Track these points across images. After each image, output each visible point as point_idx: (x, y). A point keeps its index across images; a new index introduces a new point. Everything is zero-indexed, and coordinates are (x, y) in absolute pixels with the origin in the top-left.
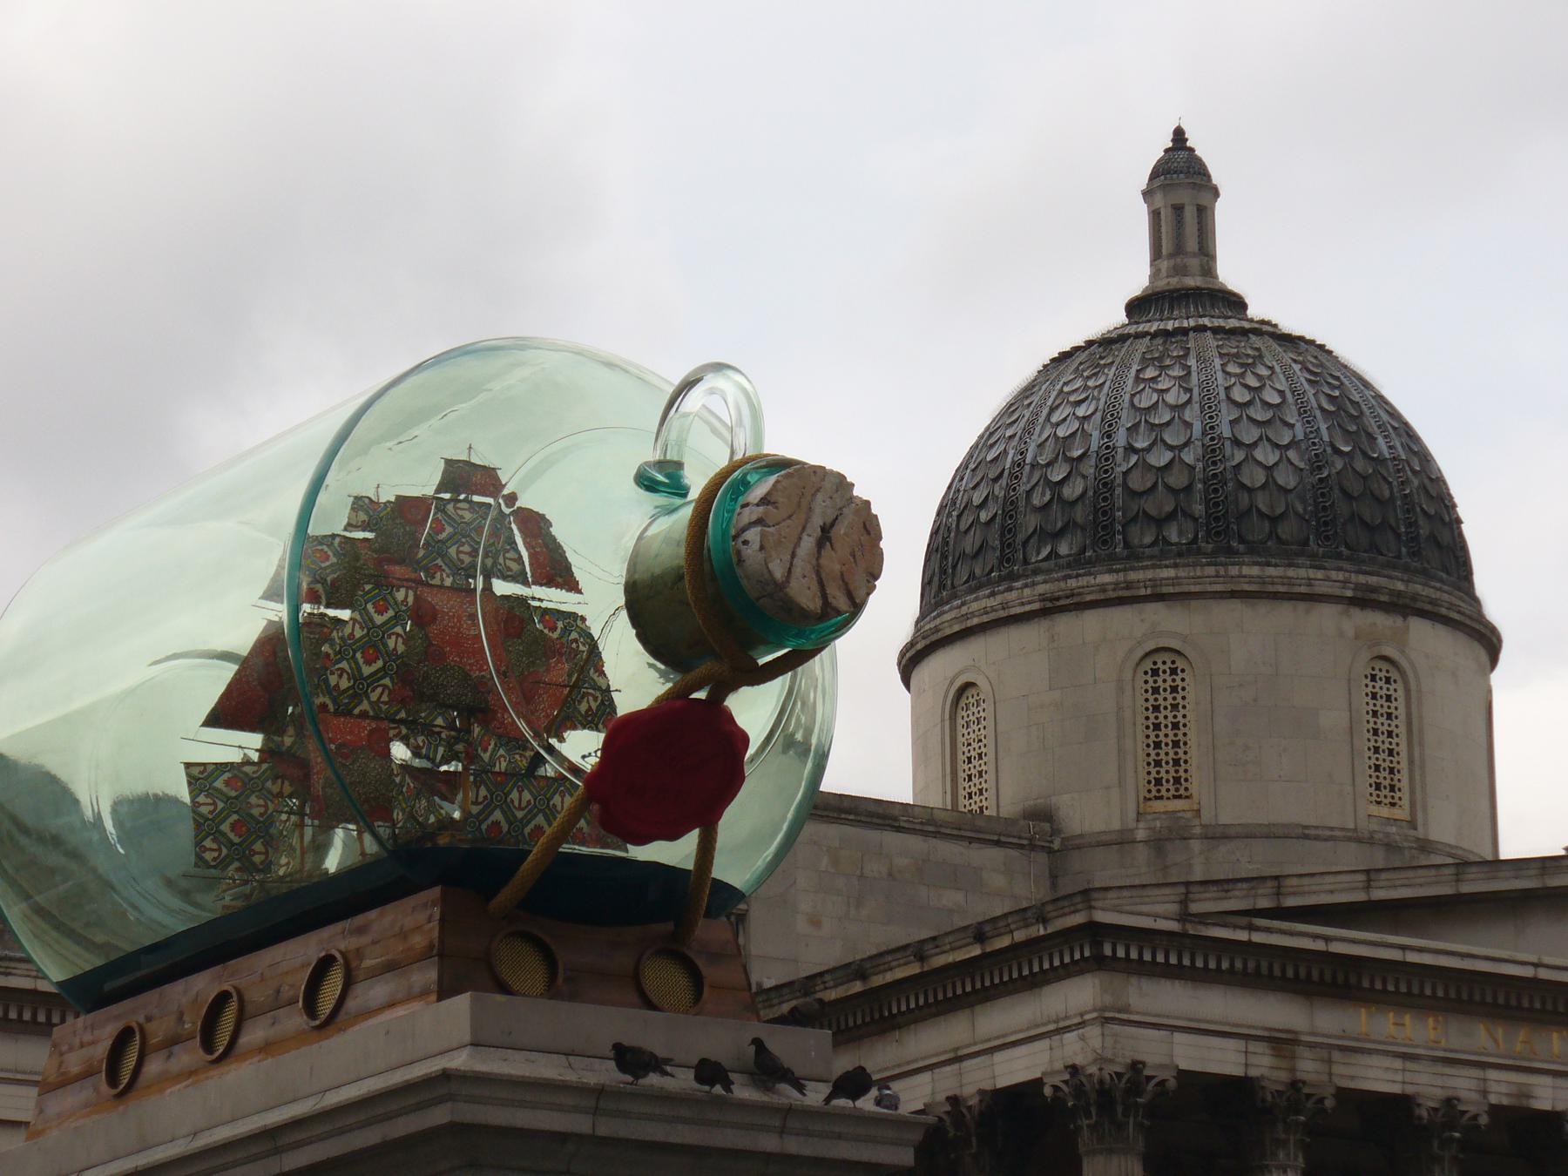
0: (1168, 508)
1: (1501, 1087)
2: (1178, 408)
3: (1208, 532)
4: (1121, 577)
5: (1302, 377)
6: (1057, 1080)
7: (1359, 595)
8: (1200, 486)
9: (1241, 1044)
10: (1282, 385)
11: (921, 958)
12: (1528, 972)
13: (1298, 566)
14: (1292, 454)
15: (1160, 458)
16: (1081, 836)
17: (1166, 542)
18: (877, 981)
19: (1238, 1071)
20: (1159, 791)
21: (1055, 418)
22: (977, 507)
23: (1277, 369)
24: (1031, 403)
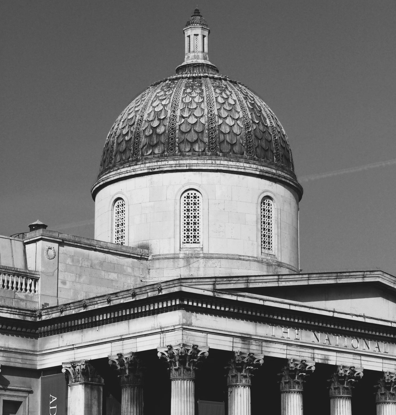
0: (195, 139)
1: (319, 356)
2: (199, 104)
3: (209, 148)
4: (177, 162)
5: (241, 96)
6: (163, 350)
7: (261, 173)
8: (207, 131)
9: (231, 339)
10: (235, 98)
11: (109, 301)
12: (331, 314)
13: (240, 162)
14: (238, 122)
15: (192, 120)
16: (160, 255)
17: (194, 151)
18: (90, 308)
19: (230, 349)
20: (188, 240)
21: (154, 104)
22: (124, 135)
23: (233, 92)
24: (145, 99)
